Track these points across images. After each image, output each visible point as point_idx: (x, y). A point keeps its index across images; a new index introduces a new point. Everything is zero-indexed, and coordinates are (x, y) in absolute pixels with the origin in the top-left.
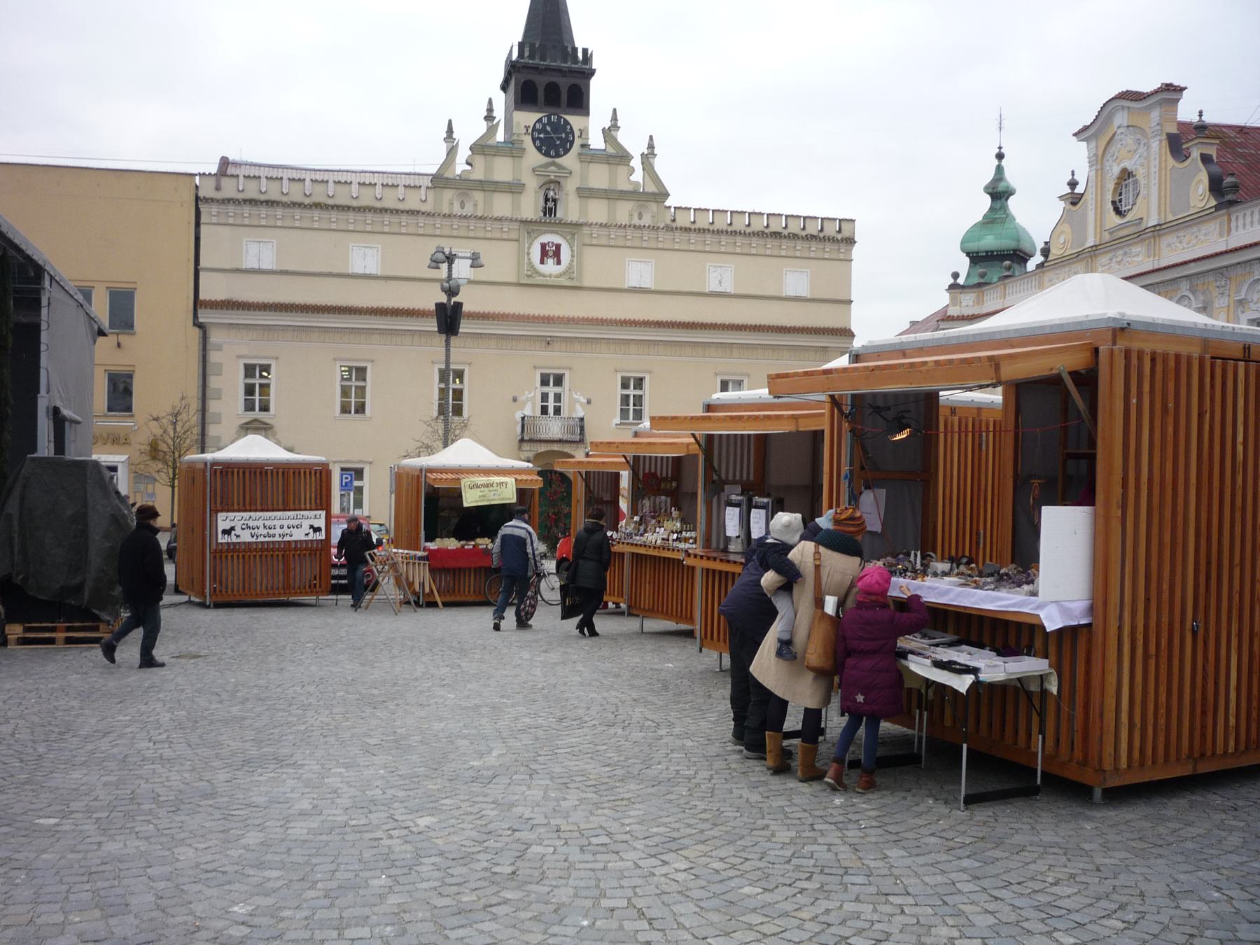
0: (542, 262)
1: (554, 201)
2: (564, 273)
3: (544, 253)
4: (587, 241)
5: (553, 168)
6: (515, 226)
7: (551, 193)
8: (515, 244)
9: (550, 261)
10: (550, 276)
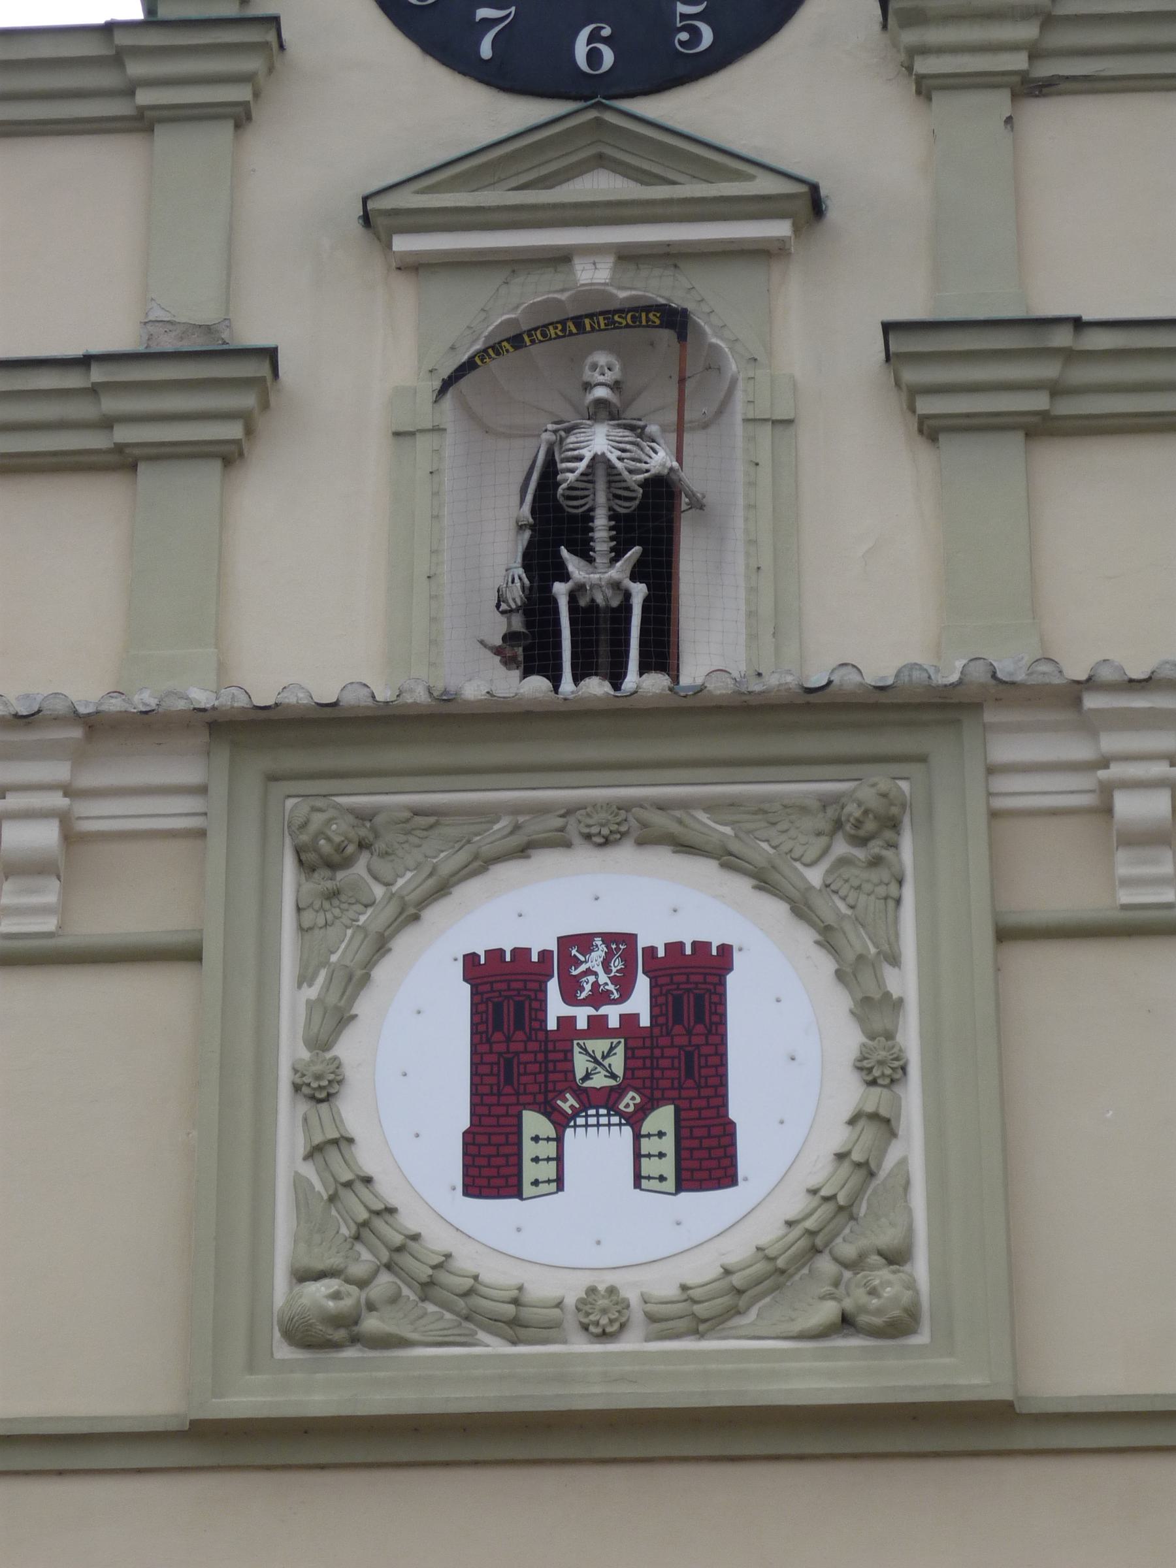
0: (492, 1167)
1: (653, 520)
2: (770, 1278)
3: (520, 1060)
4: (1059, 884)
5: (601, 185)
6: (155, 791)
7: (599, 441)
8: (160, 994)
9: (598, 1151)
10: (602, 1316)
